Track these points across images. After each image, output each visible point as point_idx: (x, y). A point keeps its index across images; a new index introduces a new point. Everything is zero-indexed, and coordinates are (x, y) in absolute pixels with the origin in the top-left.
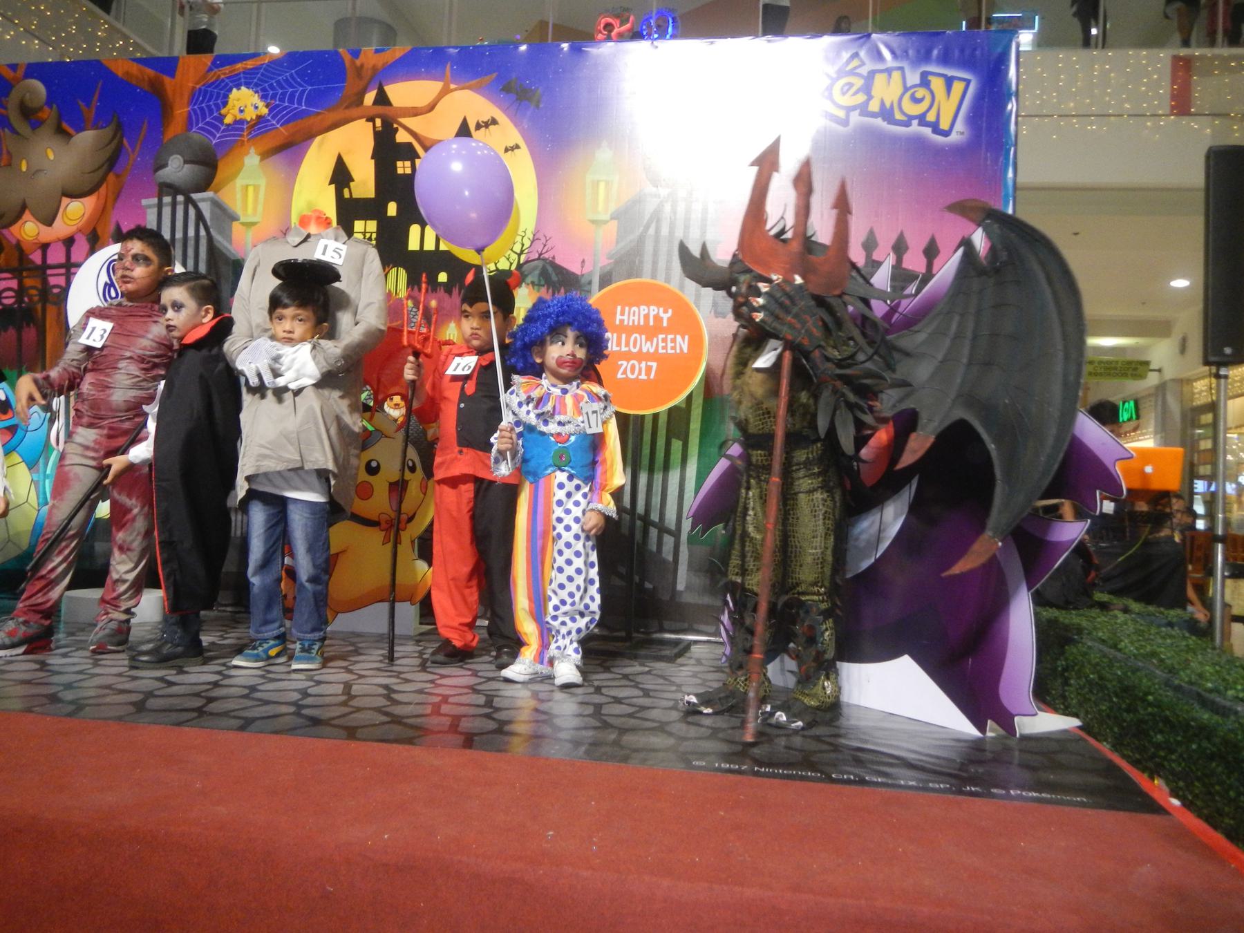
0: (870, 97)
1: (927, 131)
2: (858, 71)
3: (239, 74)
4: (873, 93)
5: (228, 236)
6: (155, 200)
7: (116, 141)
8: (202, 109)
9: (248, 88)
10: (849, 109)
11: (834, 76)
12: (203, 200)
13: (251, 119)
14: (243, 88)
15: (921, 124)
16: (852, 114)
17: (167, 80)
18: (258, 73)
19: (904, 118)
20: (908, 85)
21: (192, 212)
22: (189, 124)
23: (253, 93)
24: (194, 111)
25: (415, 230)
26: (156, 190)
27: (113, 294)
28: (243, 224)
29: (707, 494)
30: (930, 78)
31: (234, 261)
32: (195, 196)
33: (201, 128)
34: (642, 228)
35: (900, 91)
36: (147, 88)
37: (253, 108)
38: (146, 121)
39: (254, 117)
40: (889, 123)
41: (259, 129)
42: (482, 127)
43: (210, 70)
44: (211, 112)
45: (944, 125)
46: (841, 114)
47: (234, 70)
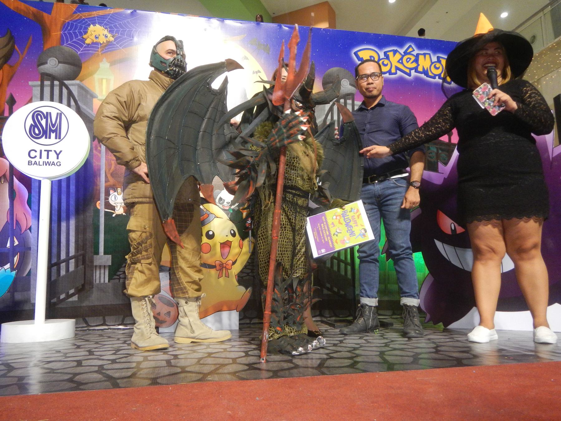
0: (418, 65)
2: (412, 53)
3: (95, 17)
4: (419, 63)
6: (39, 83)
7: (10, 45)
8: (70, 34)
9: (100, 26)
10: (411, 69)
11: (403, 54)
12: (73, 85)
13: (103, 42)
14: (97, 25)
16: (412, 71)
17: (45, 15)
18: (107, 18)
19: (433, 75)
21: (65, 91)
22: (62, 41)
23: (104, 28)
24: (65, 34)
26: (40, 76)
27: (37, 132)
30: (441, 59)
32: (66, 82)
33: (69, 44)
34: (324, 116)
35: (430, 64)
36: (30, 18)
38: (31, 37)
39: (105, 42)
40: (427, 77)
41: (109, 48)
43: (75, 13)
44: (76, 36)
46: (408, 71)
47: (90, 15)
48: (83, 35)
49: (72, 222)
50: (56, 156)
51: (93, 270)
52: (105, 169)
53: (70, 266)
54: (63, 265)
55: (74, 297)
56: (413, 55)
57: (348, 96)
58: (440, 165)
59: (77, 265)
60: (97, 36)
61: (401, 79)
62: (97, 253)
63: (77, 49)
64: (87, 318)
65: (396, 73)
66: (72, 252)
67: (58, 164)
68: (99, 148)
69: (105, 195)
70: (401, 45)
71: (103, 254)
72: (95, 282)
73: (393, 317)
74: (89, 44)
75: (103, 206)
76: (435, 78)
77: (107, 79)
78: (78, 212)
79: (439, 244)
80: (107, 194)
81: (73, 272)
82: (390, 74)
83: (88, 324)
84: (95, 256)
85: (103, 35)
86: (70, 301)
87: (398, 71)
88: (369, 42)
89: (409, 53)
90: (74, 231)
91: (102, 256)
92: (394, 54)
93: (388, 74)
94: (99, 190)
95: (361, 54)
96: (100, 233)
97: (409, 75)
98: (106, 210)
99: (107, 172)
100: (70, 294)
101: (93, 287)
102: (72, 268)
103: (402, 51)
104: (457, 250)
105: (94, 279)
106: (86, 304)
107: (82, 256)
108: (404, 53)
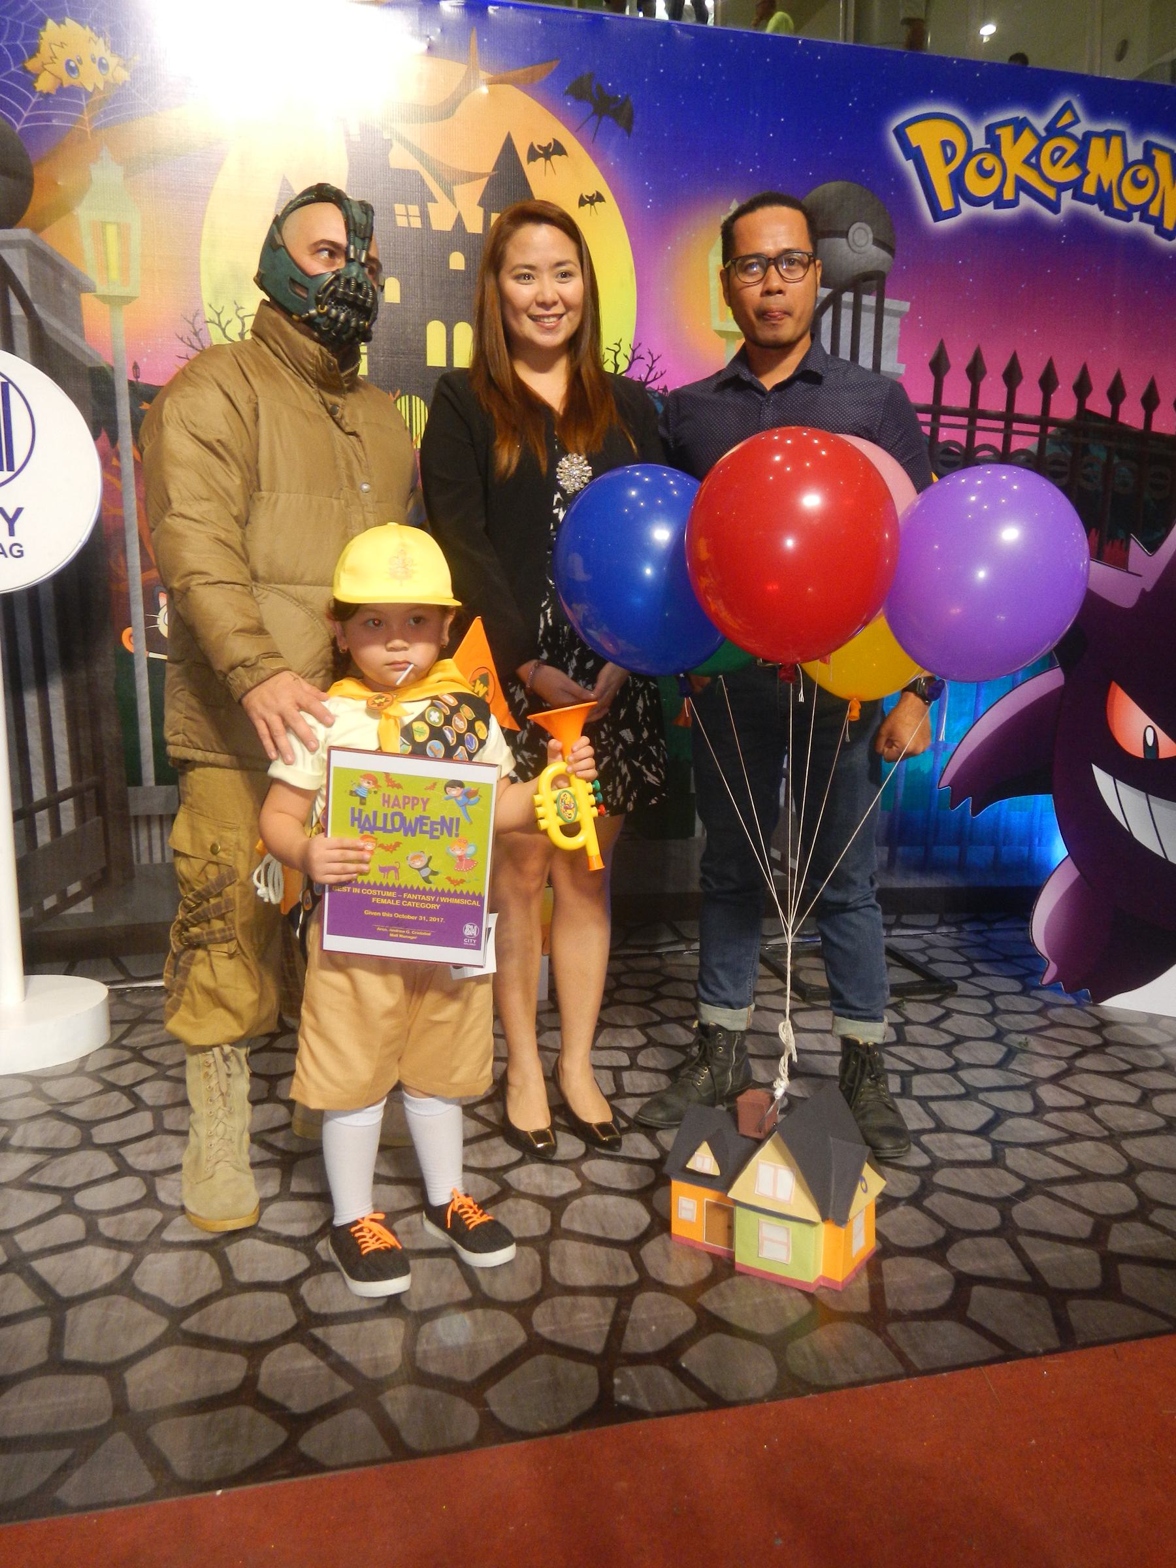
0: (1086, 173)
1: (1149, 229)
2: (1071, 130)
5: (75, 321)
10: (1061, 187)
11: (1043, 134)
12: (11, 244)
14: (68, 21)
15: (1142, 219)
19: (1124, 208)
20: (1131, 159)
25: (435, 332)
28: (105, 299)
29: (972, 756)
30: (1155, 152)
31: (92, 370)
37: (96, 66)
40: (1106, 214)
42: (540, 156)
45: (1168, 225)
46: (1050, 193)
48: (24, 61)
49: (56, 693)
50: (5, 525)
51: (129, 829)
52: (139, 525)
53: (63, 817)
54: (42, 816)
55: (82, 903)
56: (1072, 137)
57: (868, 283)
58: (1136, 548)
59: (81, 818)
60: (72, 64)
61: (1029, 222)
62: (135, 779)
63: (10, 112)
64: (124, 960)
65: (1014, 203)
66: (65, 780)
67: (15, 549)
68: (115, 462)
69: (145, 613)
70: (1039, 104)
71: (152, 783)
72: (139, 860)
73: (938, 931)
74: (48, 95)
75: (142, 644)
76: (1128, 218)
77: (118, 224)
78: (69, 663)
79: (1103, 780)
80: (151, 607)
81: (73, 834)
82: (997, 207)
83: (129, 974)
84: (131, 789)
85: (93, 60)
86: (73, 916)
87: (1022, 195)
88: (944, 93)
89: (1063, 132)
90: (64, 718)
91: (151, 787)
92: (1017, 136)
93: (991, 204)
94: (126, 598)
95: (916, 135)
96: (140, 721)
97: (1054, 207)
98: (152, 655)
99: (145, 541)
100: (70, 894)
101: (132, 876)
102: (68, 823)
103: (1040, 123)
104: (1152, 805)
105: (134, 852)
106: (118, 920)
107: (93, 791)
108: (1047, 129)
